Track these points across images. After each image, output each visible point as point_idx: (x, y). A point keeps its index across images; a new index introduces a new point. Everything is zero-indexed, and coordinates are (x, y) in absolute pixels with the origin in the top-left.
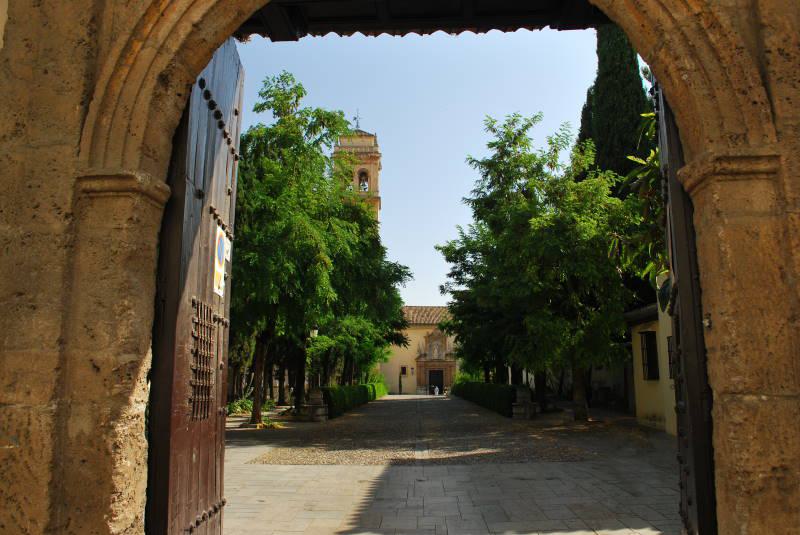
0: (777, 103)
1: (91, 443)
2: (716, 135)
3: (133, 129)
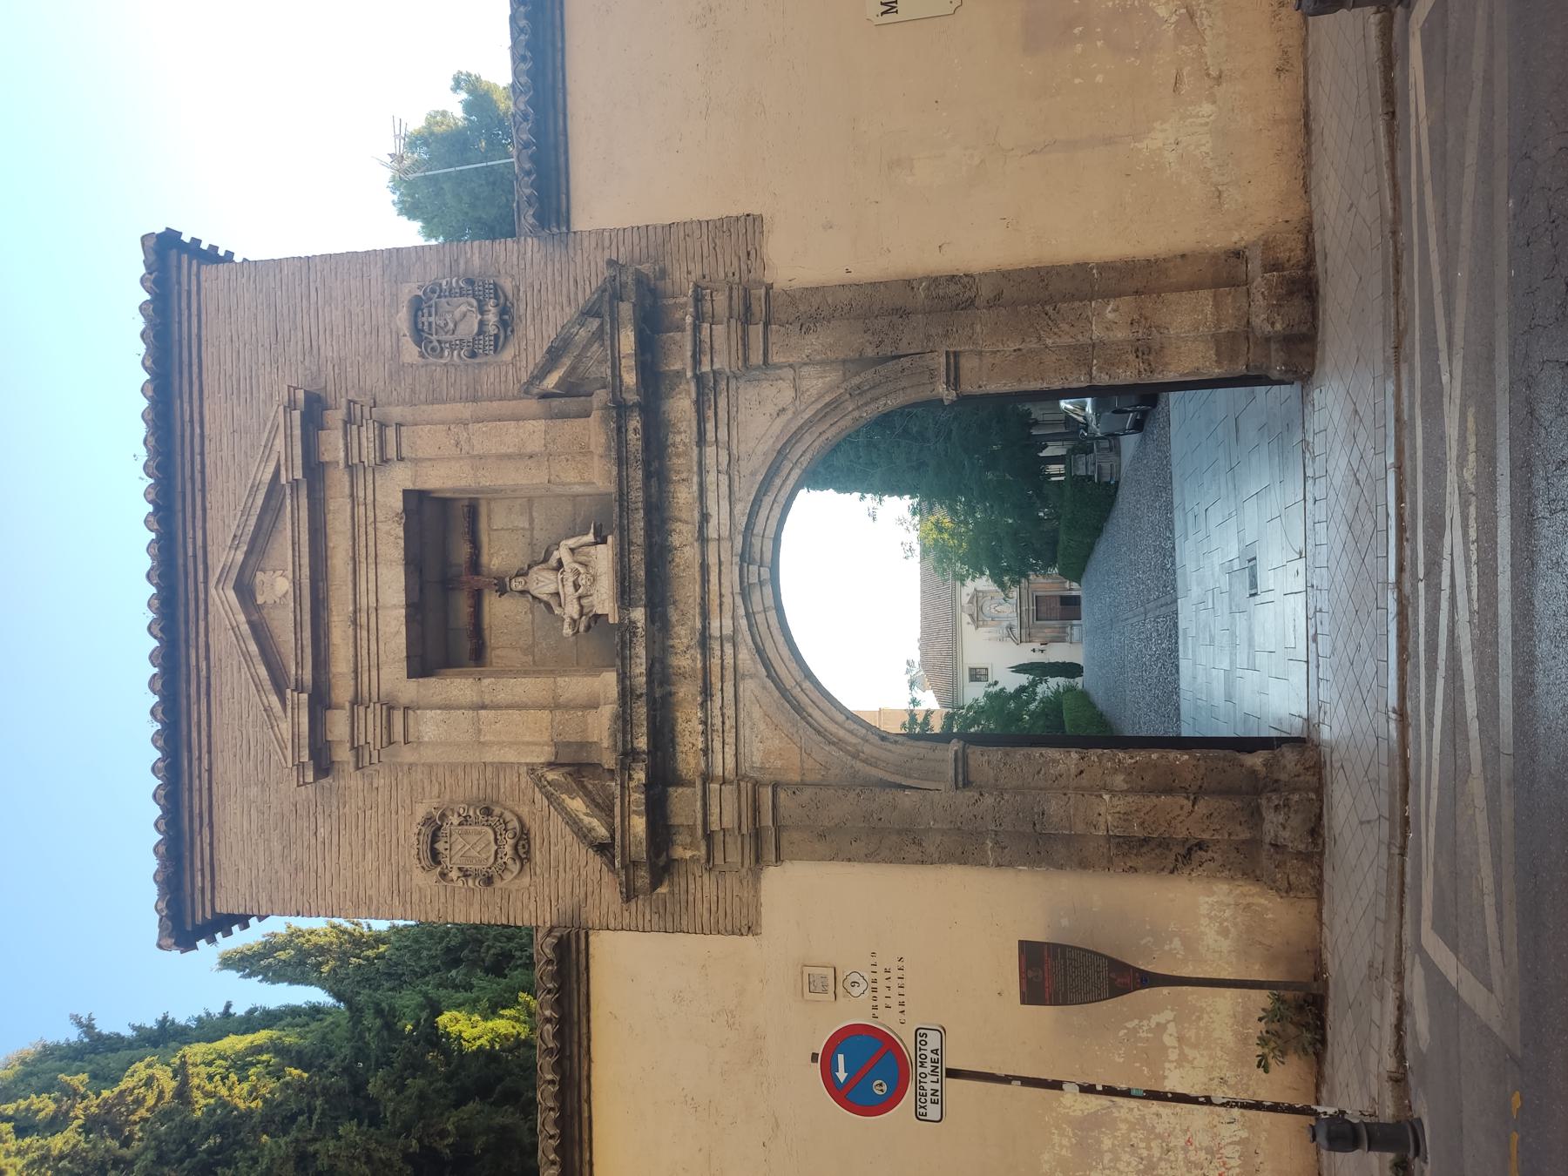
0: (912, 351)
2: (930, 387)
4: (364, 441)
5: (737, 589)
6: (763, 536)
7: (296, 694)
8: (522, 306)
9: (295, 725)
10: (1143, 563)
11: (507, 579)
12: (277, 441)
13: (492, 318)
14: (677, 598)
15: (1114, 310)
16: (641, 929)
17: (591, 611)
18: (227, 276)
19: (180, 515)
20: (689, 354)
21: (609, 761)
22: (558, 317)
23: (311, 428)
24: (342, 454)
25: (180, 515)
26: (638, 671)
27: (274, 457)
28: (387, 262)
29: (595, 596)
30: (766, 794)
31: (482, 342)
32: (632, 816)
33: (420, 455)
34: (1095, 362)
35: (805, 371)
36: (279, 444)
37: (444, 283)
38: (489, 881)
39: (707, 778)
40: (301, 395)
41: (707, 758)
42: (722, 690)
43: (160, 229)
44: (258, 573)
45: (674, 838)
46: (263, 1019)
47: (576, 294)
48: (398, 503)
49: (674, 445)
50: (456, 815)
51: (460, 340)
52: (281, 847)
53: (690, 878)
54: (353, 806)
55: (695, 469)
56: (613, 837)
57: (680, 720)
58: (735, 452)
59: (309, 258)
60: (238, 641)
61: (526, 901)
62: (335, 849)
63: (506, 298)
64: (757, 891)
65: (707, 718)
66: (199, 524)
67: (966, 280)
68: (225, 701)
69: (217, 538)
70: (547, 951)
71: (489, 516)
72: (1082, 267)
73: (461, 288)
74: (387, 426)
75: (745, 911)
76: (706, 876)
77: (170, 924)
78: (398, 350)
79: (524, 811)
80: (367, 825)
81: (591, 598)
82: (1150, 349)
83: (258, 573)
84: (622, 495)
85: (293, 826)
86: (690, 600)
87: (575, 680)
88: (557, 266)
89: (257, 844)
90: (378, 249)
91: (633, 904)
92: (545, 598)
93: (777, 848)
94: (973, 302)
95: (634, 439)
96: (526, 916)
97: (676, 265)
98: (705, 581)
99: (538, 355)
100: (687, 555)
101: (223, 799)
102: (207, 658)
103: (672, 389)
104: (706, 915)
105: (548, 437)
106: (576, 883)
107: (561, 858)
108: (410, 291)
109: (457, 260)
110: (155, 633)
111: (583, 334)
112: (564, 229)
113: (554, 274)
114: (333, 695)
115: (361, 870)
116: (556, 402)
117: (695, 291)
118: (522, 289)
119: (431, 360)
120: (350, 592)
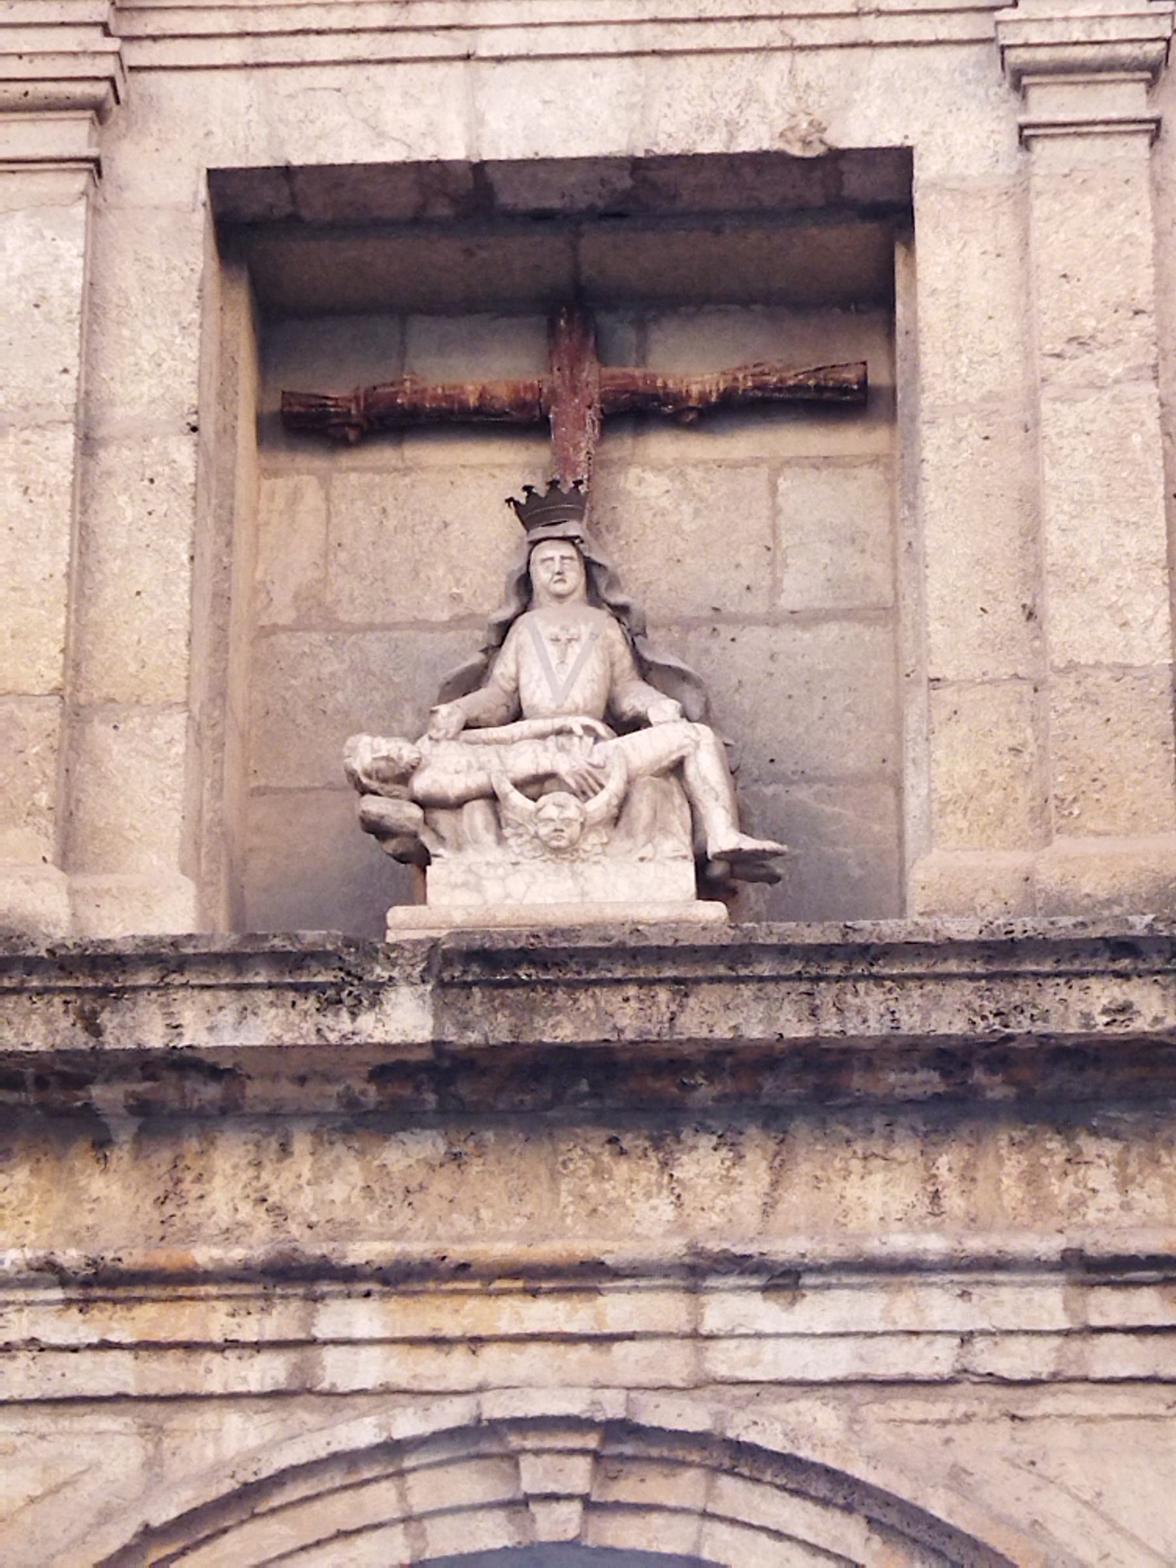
5: (496, 1408)
6: (705, 1515)
17: (441, 839)
29: (495, 854)
42: (105, 1346)
55: (976, 1245)
81: (489, 838)
86: (462, 1222)
87: (173, 777)
92: (503, 668)
100: (641, 1208)
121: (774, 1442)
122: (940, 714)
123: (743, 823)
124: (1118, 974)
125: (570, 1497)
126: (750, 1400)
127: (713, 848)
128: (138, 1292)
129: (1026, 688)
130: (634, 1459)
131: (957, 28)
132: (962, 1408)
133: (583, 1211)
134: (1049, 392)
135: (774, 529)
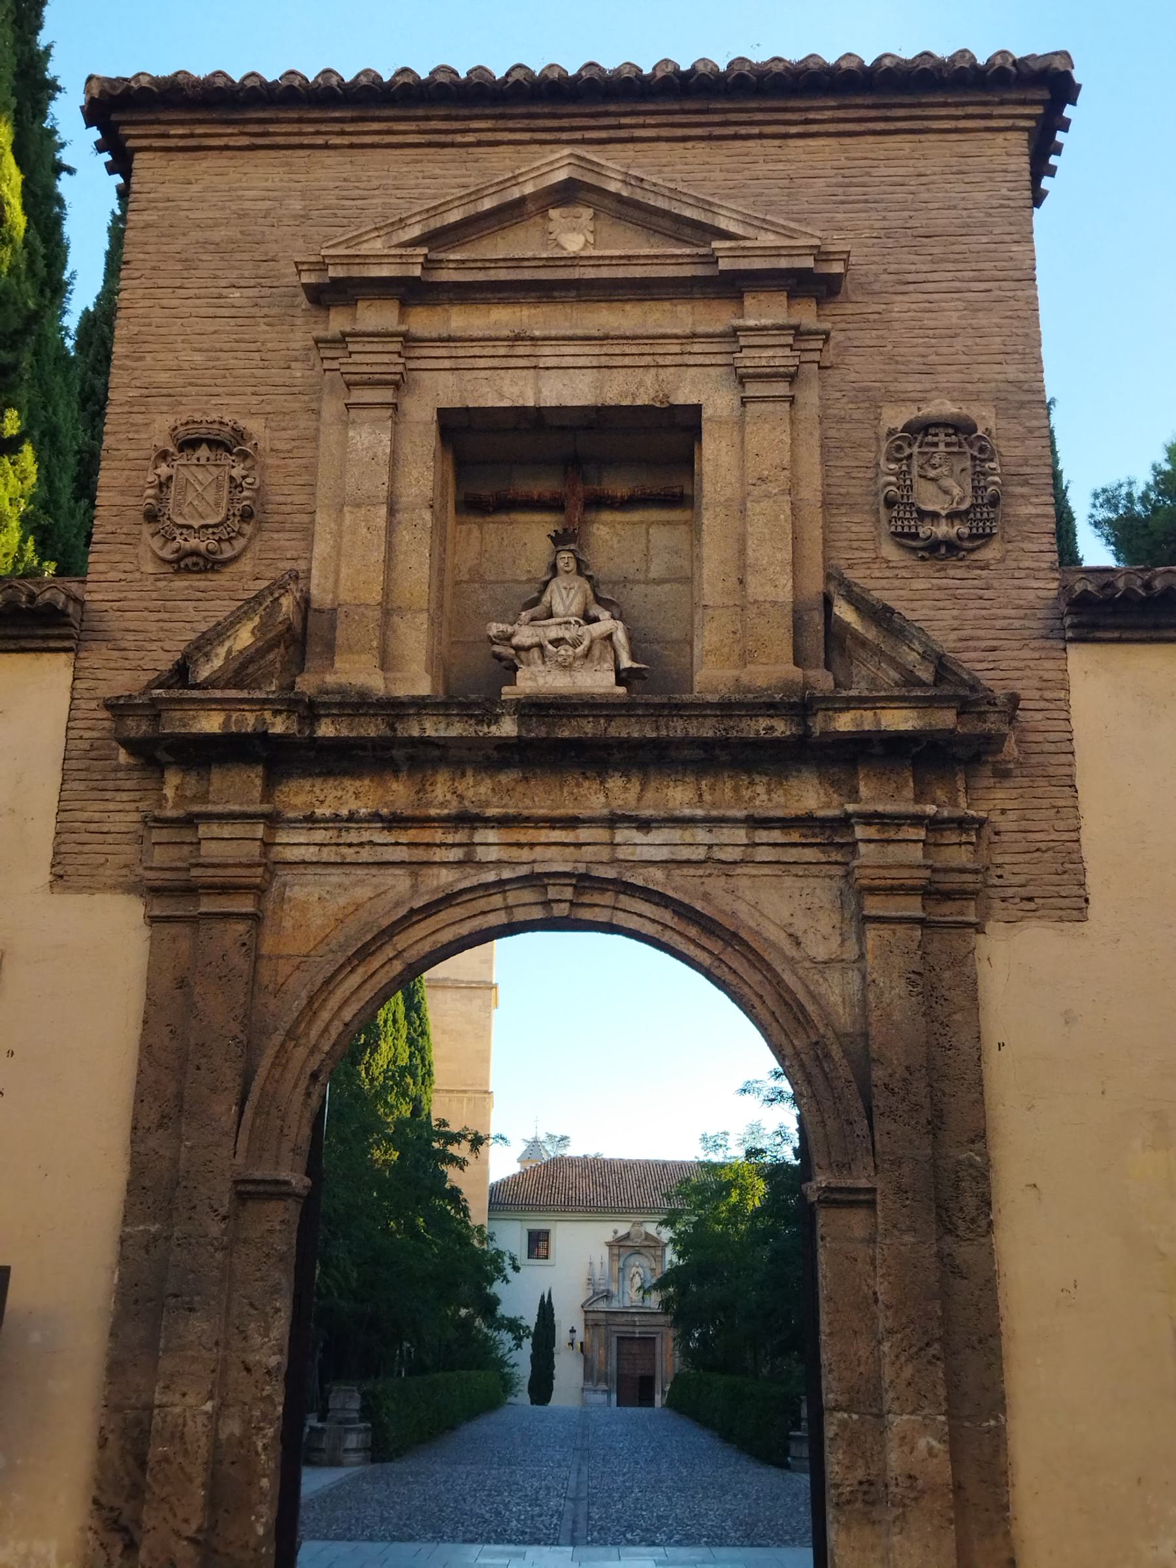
0: (877, 1138)
1: (241, 1444)
2: (824, 1163)
3: (286, 1131)
4: (770, 353)
5: (539, 869)
6: (614, 908)
7: (421, 260)
8: (959, 573)
9: (379, 259)
10: (651, 1499)
11: (572, 547)
12: (771, 236)
13: (943, 530)
14: (533, 783)
15: (930, 1450)
16: (71, 724)
18: (1012, 168)
19: (676, 107)
20: (880, 808)
21: (307, 684)
22: (941, 623)
23: (790, 282)
24: (751, 323)
25: (676, 107)
26: (428, 725)
27: (750, 232)
28: (1026, 387)
29: (542, 668)
30: (245, 905)
31: (908, 515)
32: (223, 714)
33: (748, 429)
34: (855, 1417)
35: (854, 977)
36: (768, 239)
37: (993, 465)
38: (151, 516)
39: (273, 820)
40: (837, 268)
41: (300, 821)
42: (397, 844)
43: (1077, 76)
44: (591, 211)
45: (194, 773)
46: (48, 217)
47: (975, 649)
48: (685, 396)
49: (752, 783)
50: (244, 473)
51: (911, 486)
52: (218, 240)
53: (137, 795)
54: (268, 336)
55: (714, 813)
56: (196, 686)
57: (358, 783)
58: (739, 871)
59: (1034, 280)
60: (497, 184)
61: (121, 566)
62: (211, 311)
63: (971, 551)
64: (113, 888)
65: (357, 822)
66: (665, 132)
67: (983, 1223)
68: (419, 167)
69: (646, 157)
70: (48, 595)
71: (669, 523)
72: (998, 1404)
73: (986, 488)
74: (791, 383)
75: (84, 870)
76: (137, 817)
77: (119, 92)
78: (901, 400)
79: (246, 565)
80: (240, 355)
81: (540, 662)
82: (873, 1503)
83: (591, 211)
84: (677, 709)
85: (246, 256)
86: (527, 802)
88: (1017, 624)
89: (223, 209)
90: (1045, 375)
91: (106, 714)
93: (168, 919)
94: (950, 1232)
95: (758, 727)
96: (101, 567)
97: (1015, 793)
98: (554, 823)
99: (882, 593)
100: (593, 798)
101: (288, 164)
102: (479, 144)
103: (832, 785)
104: (85, 816)
105: (768, 605)
106: (141, 637)
107: (175, 616)
108: (984, 418)
109: (1026, 483)
110: (513, 73)
111: (911, 658)
112: (1069, 634)
113: (1005, 618)
114: (419, 309)
115: (180, 346)
116: (818, 618)
117: (973, 820)
118: (984, 573)
119: (884, 446)
120: (562, 333)
121: (640, 882)
122: (707, 618)
123: (633, 658)
124: (769, 716)
125: (565, 901)
126: (632, 867)
127: (622, 667)
128: (409, 825)
129: (739, 609)
130: (589, 888)
131: (719, 359)
132: (708, 872)
133: (572, 798)
134: (751, 498)
135: (647, 548)
